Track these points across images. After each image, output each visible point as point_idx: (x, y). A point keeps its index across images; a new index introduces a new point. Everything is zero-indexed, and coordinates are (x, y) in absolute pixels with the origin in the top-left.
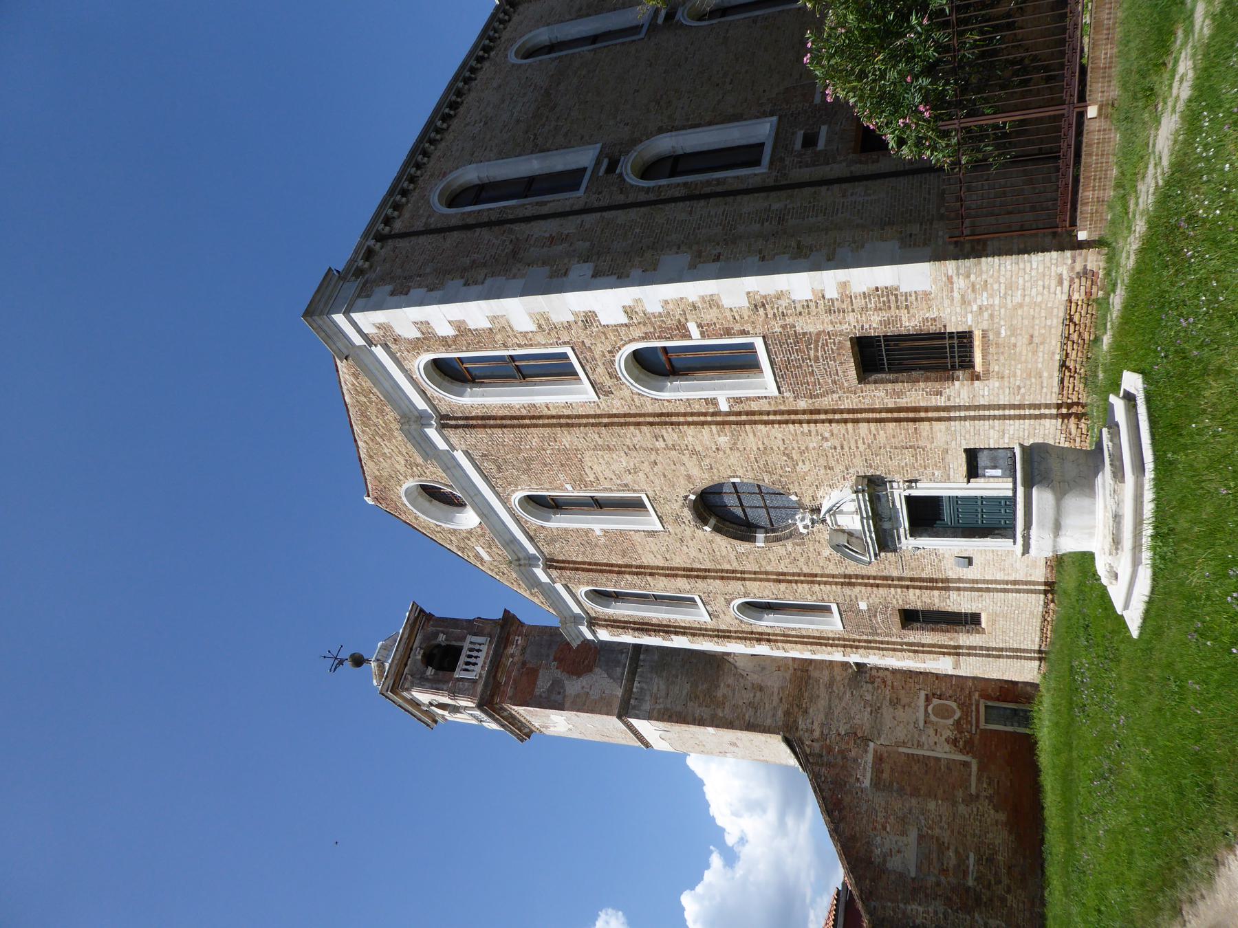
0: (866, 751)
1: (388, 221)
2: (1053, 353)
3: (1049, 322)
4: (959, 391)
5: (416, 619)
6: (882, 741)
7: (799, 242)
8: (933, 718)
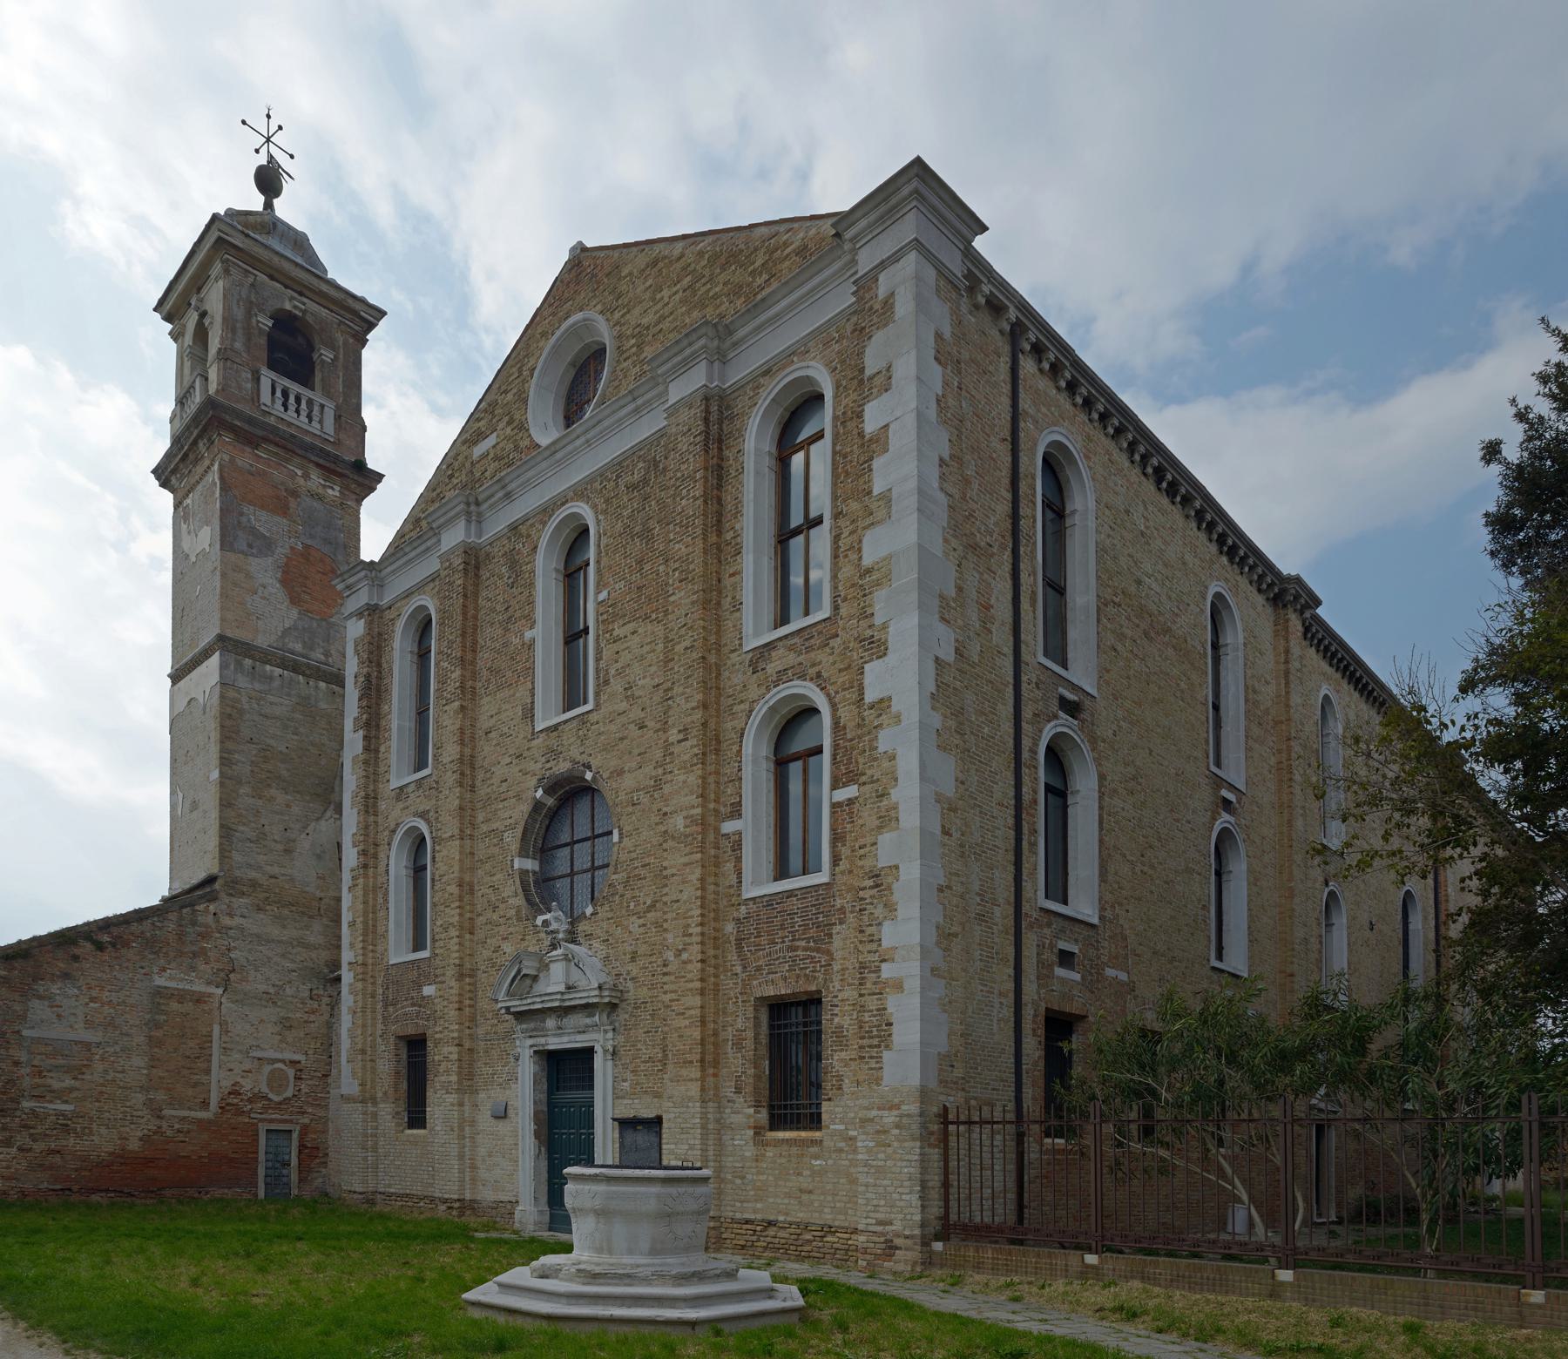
0: (209, 983)
5: (355, 313)
6: (226, 1004)
8: (267, 1069)
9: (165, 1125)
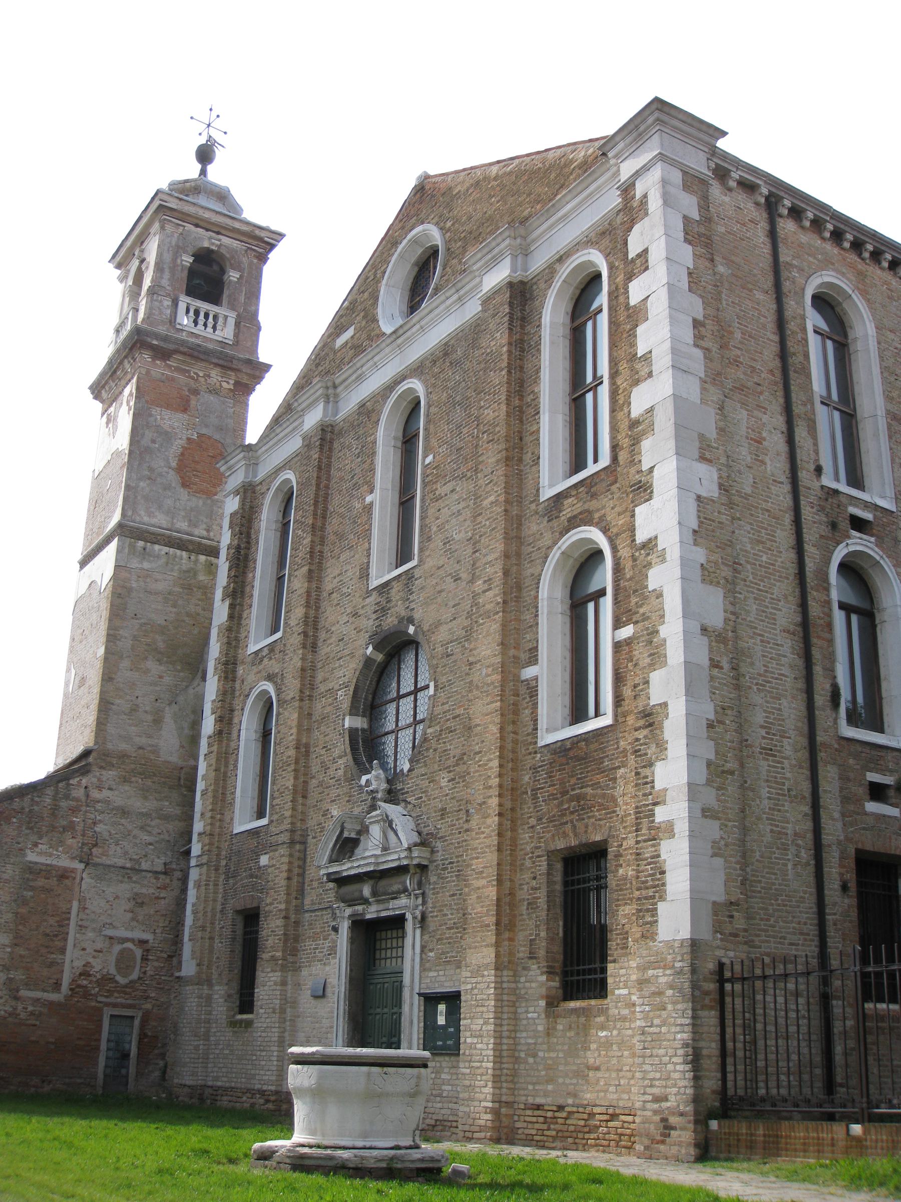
0: (73, 858)
1: (796, 213)
2: (575, 1096)
3: (612, 1089)
4: (538, 981)
5: (261, 240)
6: (87, 880)
7: (732, 773)
9: (20, 1007)
